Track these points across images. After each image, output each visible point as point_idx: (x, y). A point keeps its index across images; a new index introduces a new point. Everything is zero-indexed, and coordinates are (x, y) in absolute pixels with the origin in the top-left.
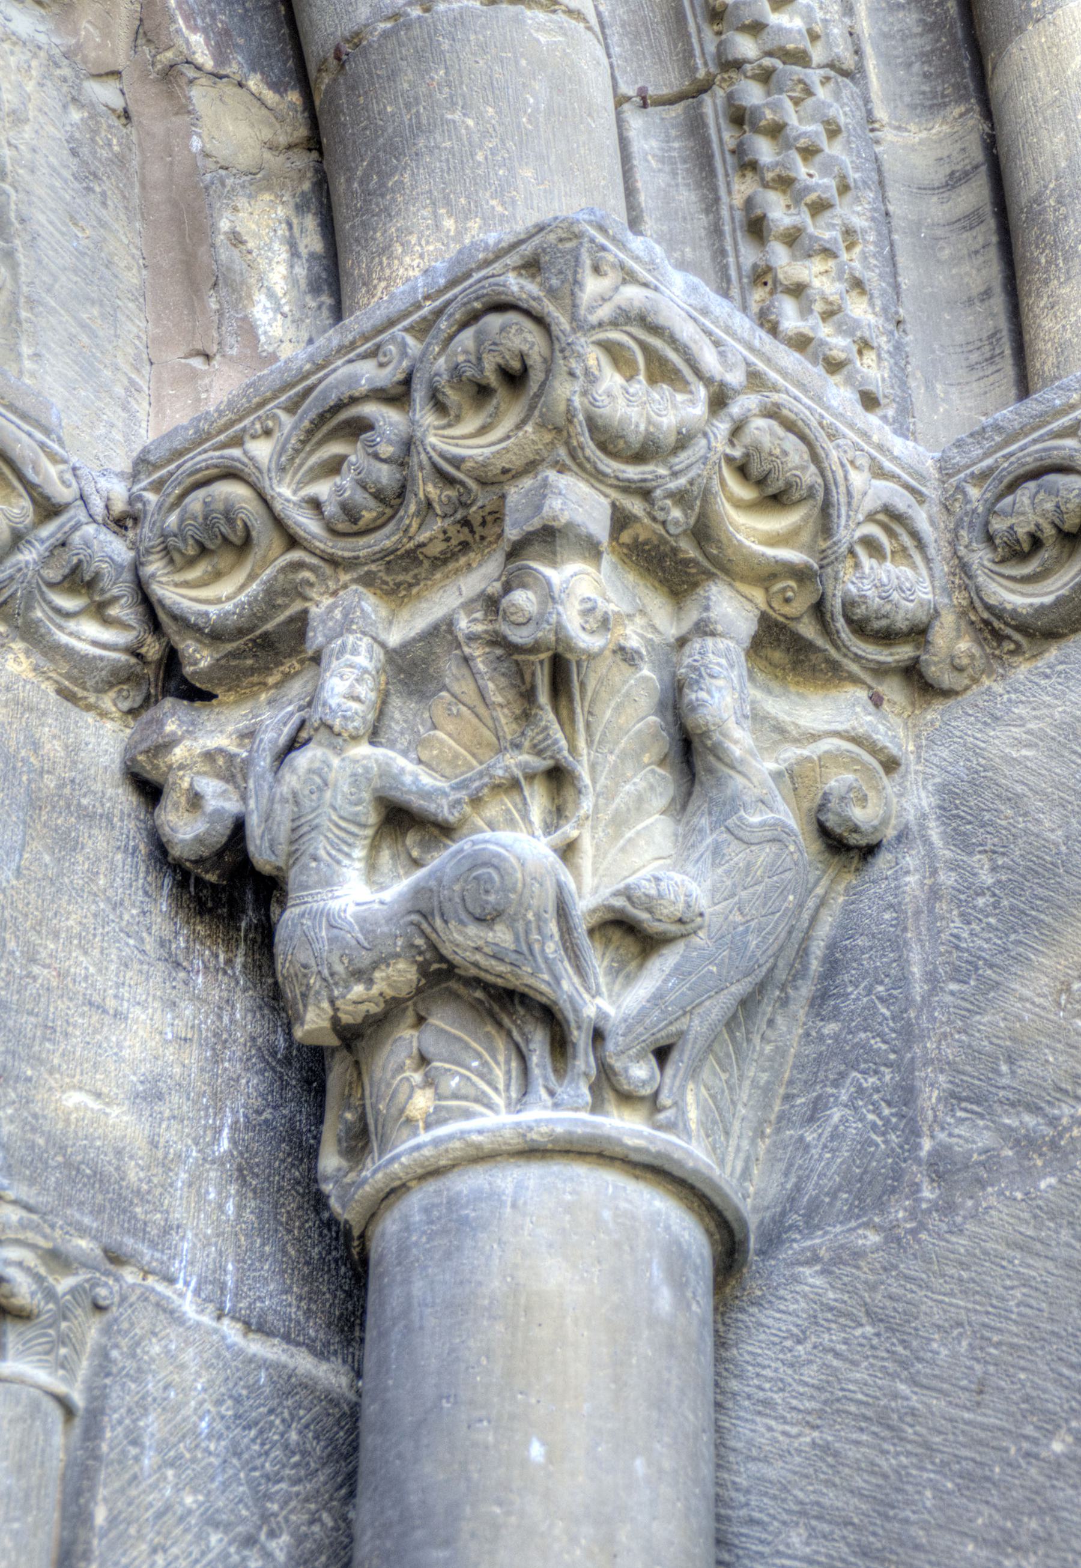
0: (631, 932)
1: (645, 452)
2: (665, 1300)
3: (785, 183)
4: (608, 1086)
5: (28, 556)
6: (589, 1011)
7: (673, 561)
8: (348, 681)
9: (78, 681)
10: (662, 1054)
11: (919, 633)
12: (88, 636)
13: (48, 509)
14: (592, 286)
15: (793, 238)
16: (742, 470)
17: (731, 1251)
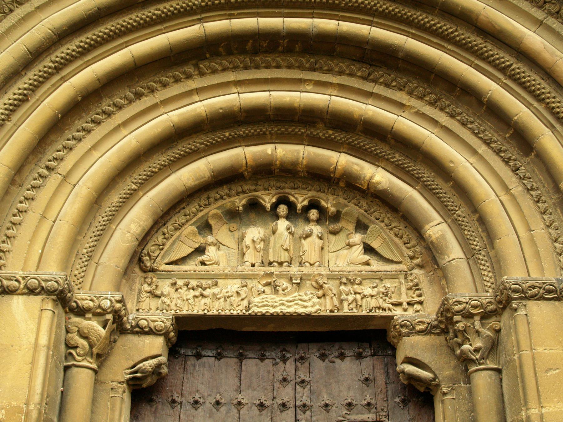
0: (477, 350)
1: (462, 311)
2: (489, 380)
3: (481, 264)
4: (480, 364)
5: (429, 328)
6: (475, 358)
7: (469, 316)
8: (451, 334)
9: (438, 334)
10: (483, 359)
11: (496, 310)
12: (438, 331)
13: (428, 324)
14: (450, 301)
15: (483, 269)
16: (472, 307)
17: (499, 371)
